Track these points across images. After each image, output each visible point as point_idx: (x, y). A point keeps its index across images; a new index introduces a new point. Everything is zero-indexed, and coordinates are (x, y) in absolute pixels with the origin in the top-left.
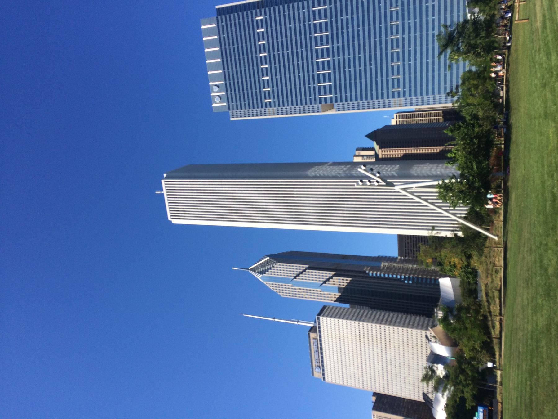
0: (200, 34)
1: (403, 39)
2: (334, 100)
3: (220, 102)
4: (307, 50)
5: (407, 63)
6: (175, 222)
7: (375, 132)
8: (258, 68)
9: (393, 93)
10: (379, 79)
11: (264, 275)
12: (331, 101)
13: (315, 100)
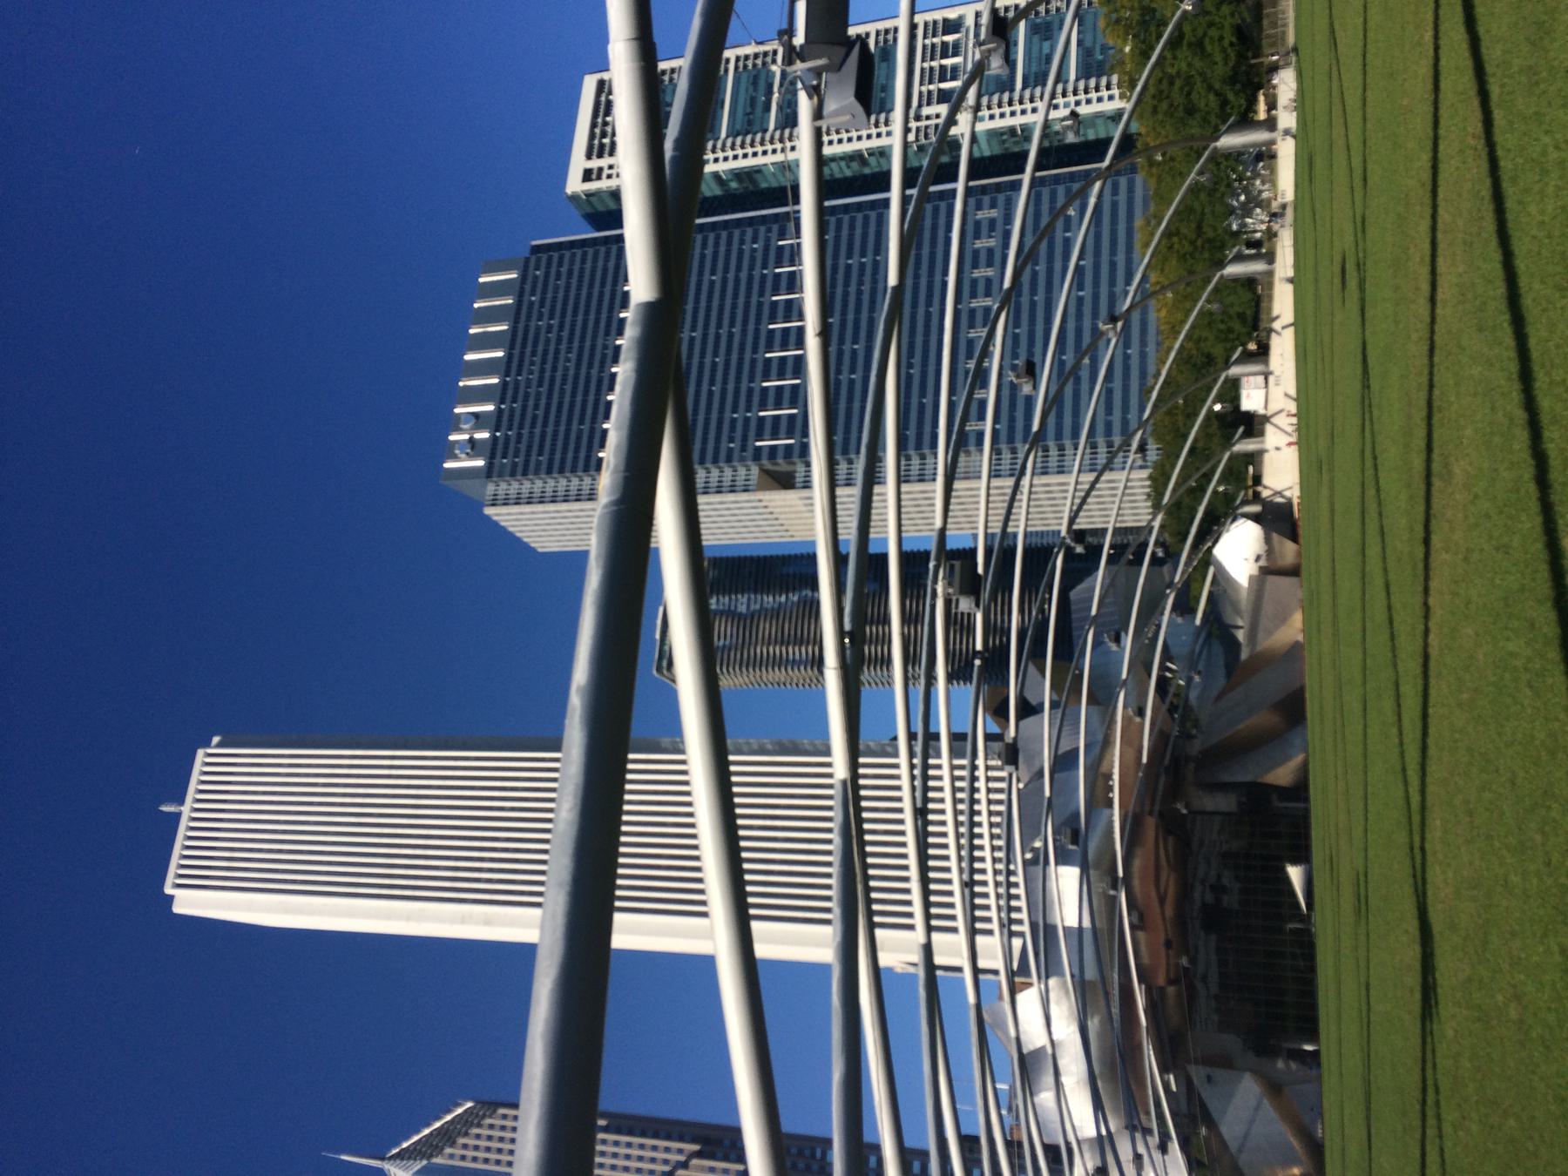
2: (796, 452)
3: (470, 456)
4: (744, 331)
13: (744, 448)
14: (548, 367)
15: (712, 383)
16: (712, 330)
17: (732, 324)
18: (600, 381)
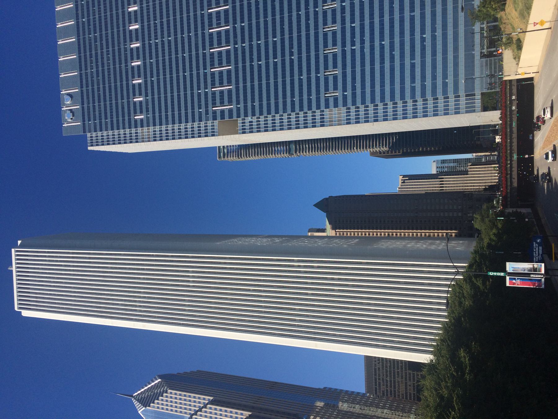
1: (343, 9)
4: (196, 35)
5: (348, 48)
8: (126, 66)
10: (304, 77)
12: (231, 116)
13: (207, 112)
15: (184, 71)
16: (179, 36)
17: (189, 32)
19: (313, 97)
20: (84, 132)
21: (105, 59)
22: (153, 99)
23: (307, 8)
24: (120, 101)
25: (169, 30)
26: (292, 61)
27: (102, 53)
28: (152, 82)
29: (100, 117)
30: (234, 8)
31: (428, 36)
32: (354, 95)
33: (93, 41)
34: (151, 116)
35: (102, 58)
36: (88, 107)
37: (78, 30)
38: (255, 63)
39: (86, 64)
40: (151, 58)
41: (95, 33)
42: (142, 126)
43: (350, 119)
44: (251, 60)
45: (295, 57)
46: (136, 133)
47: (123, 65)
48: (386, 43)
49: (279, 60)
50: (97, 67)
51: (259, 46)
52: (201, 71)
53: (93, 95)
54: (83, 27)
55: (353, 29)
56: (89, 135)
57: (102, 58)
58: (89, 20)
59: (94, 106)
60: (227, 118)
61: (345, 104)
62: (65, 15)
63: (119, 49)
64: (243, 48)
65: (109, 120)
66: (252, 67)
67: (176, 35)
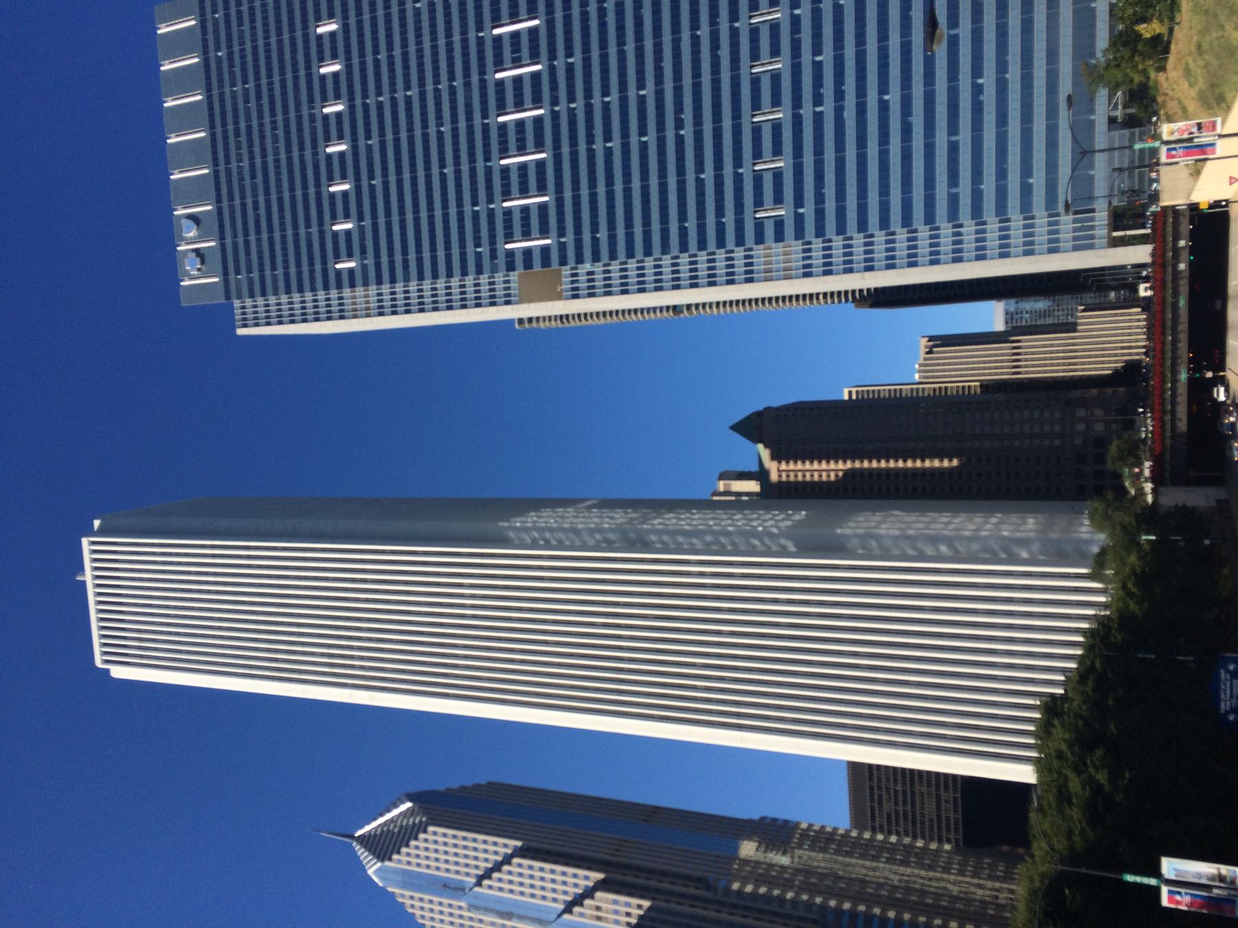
0: (152, 49)
1: (795, 22)
4: (467, 85)
5: (807, 111)
6: (118, 672)
7: (759, 414)
8: (315, 154)
9: (759, 225)
10: (708, 175)
11: (387, 863)
12: (546, 262)
13: (493, 255)
14: (257, 149)
15: (442, 165)
17: (452, 78)
18: (316, 167)
19: (729, 219)
20: (228, 297)
21: (269, 141)
22: (375, 226)
23: (714, 22)
24: (302, 231)
25: (407, 75)
26: (680, 141)
27: (261, 125)
28: (372, 189)
29: (261, 265)
30: (550, 24)
31: (988, 80)
32: (820, 214)
33: (240, 101)
34: (370, 261)
35: (262, 137)
36: (235, 245)
37: (207, 76)
38: (598, 146)
39: (227, 150)
40: (368, 137)
41: (245, 82)
42: (352, 285)
43: (810, 266)
44: (590, 139)
45: (687, 132)
46: (341, 298)
47: (308, 153)
48: (894, 97)
49: (651, 138)
50: (252, 157)
51: (606, 107)
52: (480, 164)
53: (244, 216)
54: (219, 69)
55: (818, 67)
56: (237, 303)
57: (262, 137)
58: (230, 54)
59: (247, 243)
60: (537, 267)
61: (799, 234)
62: (178, 44)
63: (299, 118)
64: (572, 114)
65: (280, 272)
66: (591, 154)
67: (422, 84)
